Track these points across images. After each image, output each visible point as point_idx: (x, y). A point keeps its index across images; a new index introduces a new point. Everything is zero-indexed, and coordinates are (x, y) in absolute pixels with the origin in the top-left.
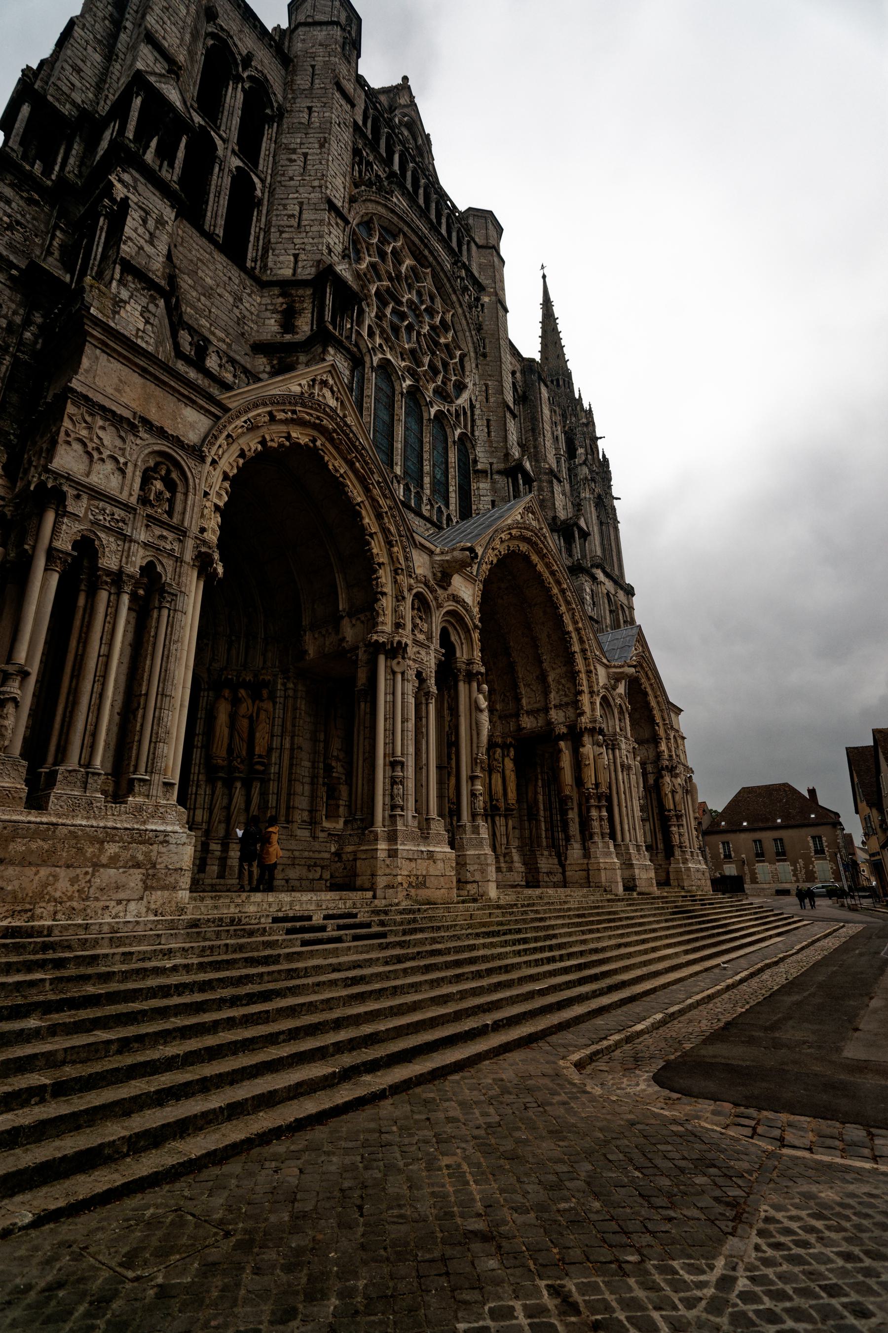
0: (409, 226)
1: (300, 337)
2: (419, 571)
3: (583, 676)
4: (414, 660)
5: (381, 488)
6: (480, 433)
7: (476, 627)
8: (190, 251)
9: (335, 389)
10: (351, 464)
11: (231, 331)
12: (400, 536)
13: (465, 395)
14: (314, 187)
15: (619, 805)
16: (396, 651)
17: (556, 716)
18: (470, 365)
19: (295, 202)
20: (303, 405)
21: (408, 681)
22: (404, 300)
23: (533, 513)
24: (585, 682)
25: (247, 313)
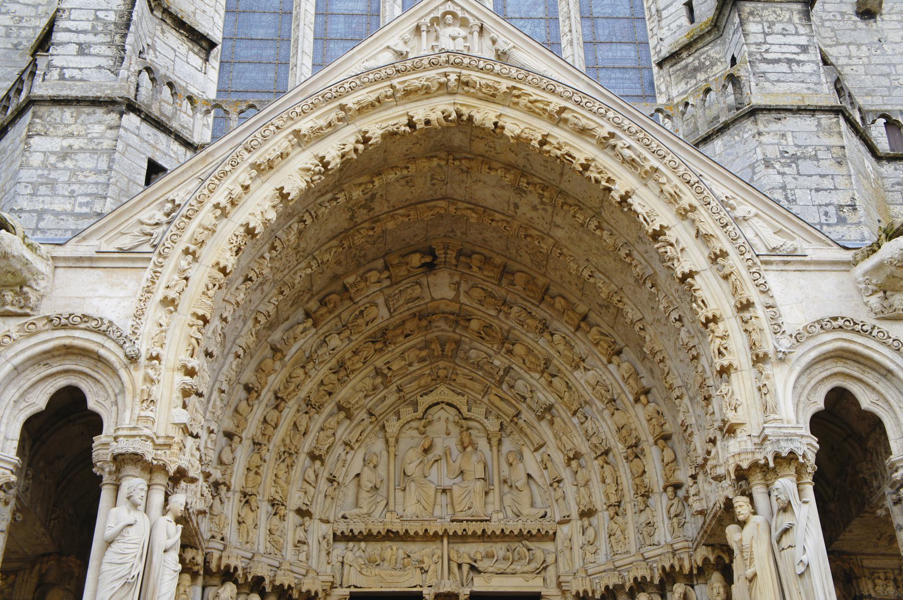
3: (730, 324)
23: (464, 23)
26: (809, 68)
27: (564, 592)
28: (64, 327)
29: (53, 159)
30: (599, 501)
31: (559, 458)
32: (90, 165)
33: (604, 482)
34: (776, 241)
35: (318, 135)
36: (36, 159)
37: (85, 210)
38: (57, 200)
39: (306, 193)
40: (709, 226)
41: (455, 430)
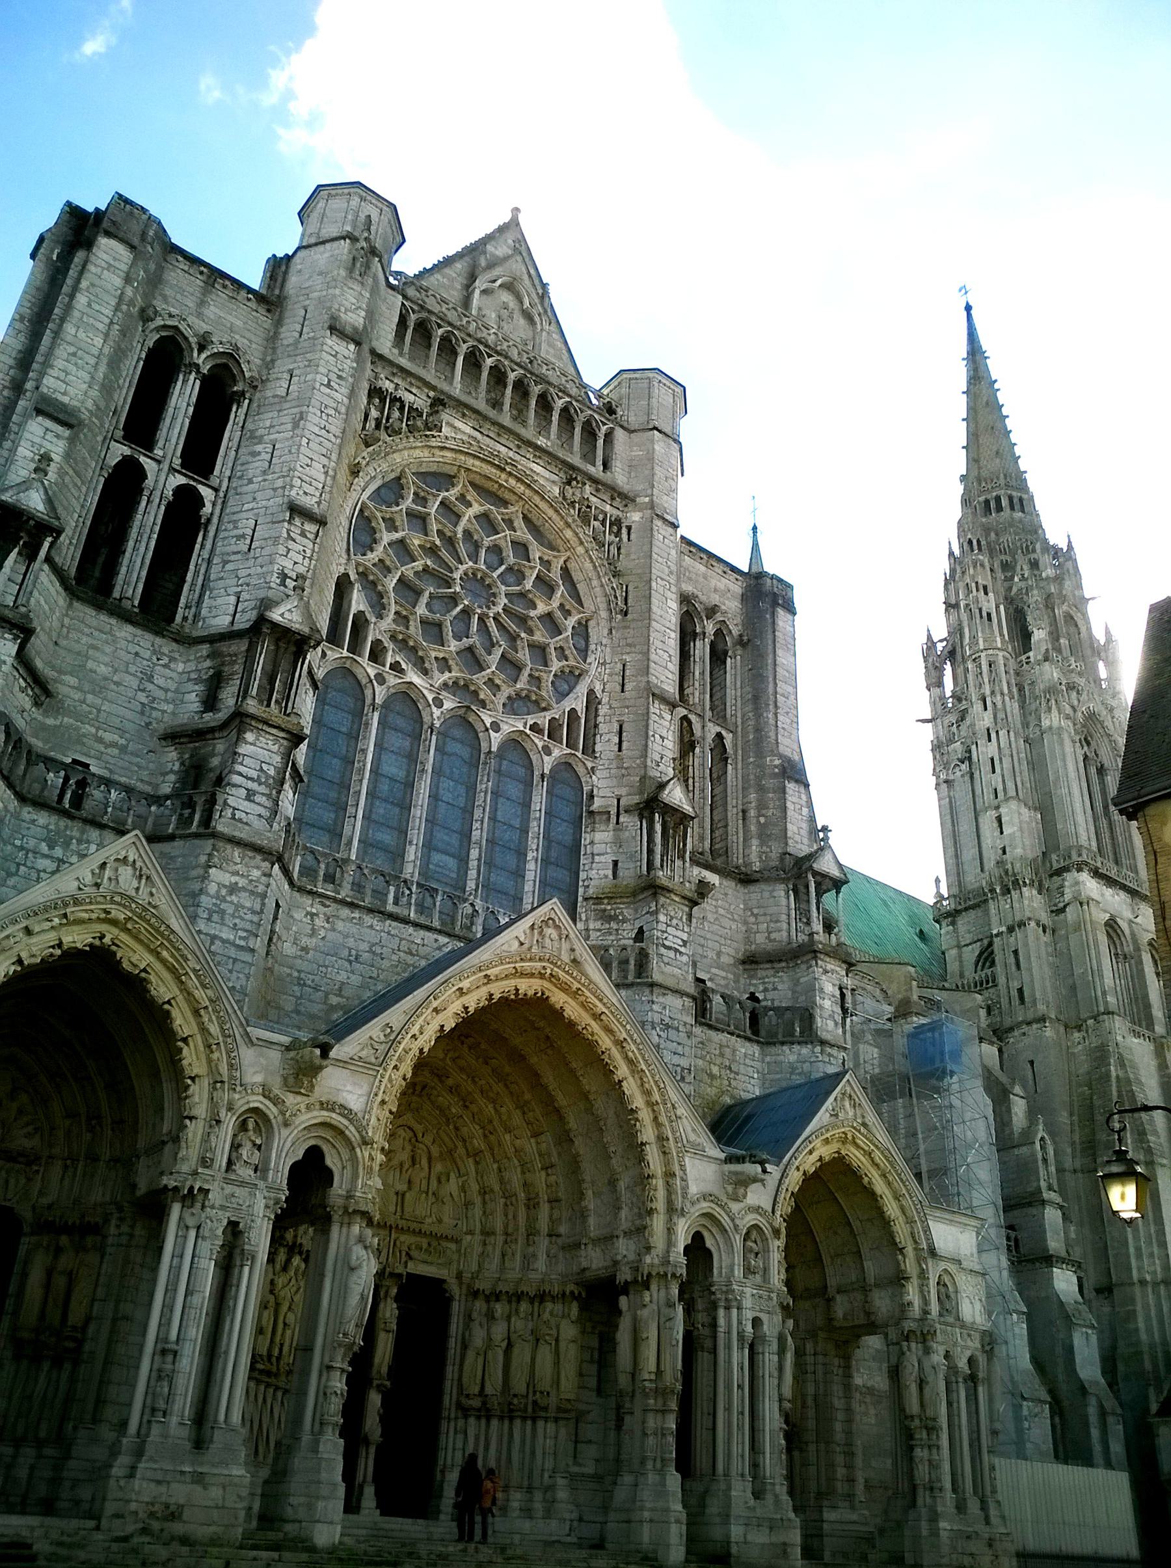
0: (475, 457)
1: (222, 716)
2: (255, 1077)
3: (659, 1183)
4: (223, 1208)
5: (198, 977)
6: (605, 744)
7: (365, 1142)
8: (78, 642)
9: (138, 864)
10: (158, 955)
11: (128, 726)
12: (225, 1036)
13: (582, 689)
14: (275, 490)
15: (728, 1409)
16: (190, 1198)
17: (625, 1248)
18: (598, 632)
19: (250, 515)
20: (76, 902)
21: (204, 1238)
22: (457, 575)
23: (557, 927)
24: (661, 1194)
25: (160, 694)
26: (685, 959)
27: (461, 1284)
28: (328, 1110)
29: (224, 892)
30: (499, 1226)
31: (475, 1187)
32: (248, 905)
33: (506, 1215)
34: (692, 1137)
35: (469, 991)
36: (212, 888)
37: (242, 943)
38: (225, 929)
39: (453, 1030)
40: (663, 1119)
41: (408, 1148)
